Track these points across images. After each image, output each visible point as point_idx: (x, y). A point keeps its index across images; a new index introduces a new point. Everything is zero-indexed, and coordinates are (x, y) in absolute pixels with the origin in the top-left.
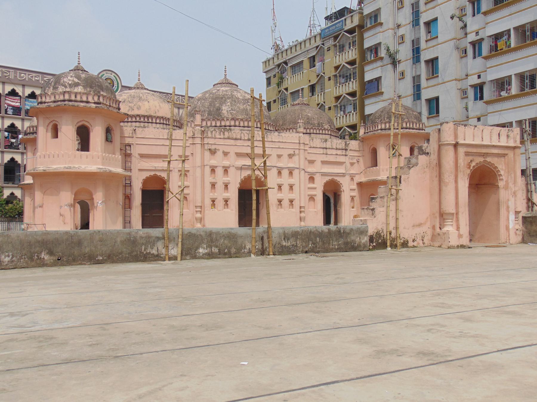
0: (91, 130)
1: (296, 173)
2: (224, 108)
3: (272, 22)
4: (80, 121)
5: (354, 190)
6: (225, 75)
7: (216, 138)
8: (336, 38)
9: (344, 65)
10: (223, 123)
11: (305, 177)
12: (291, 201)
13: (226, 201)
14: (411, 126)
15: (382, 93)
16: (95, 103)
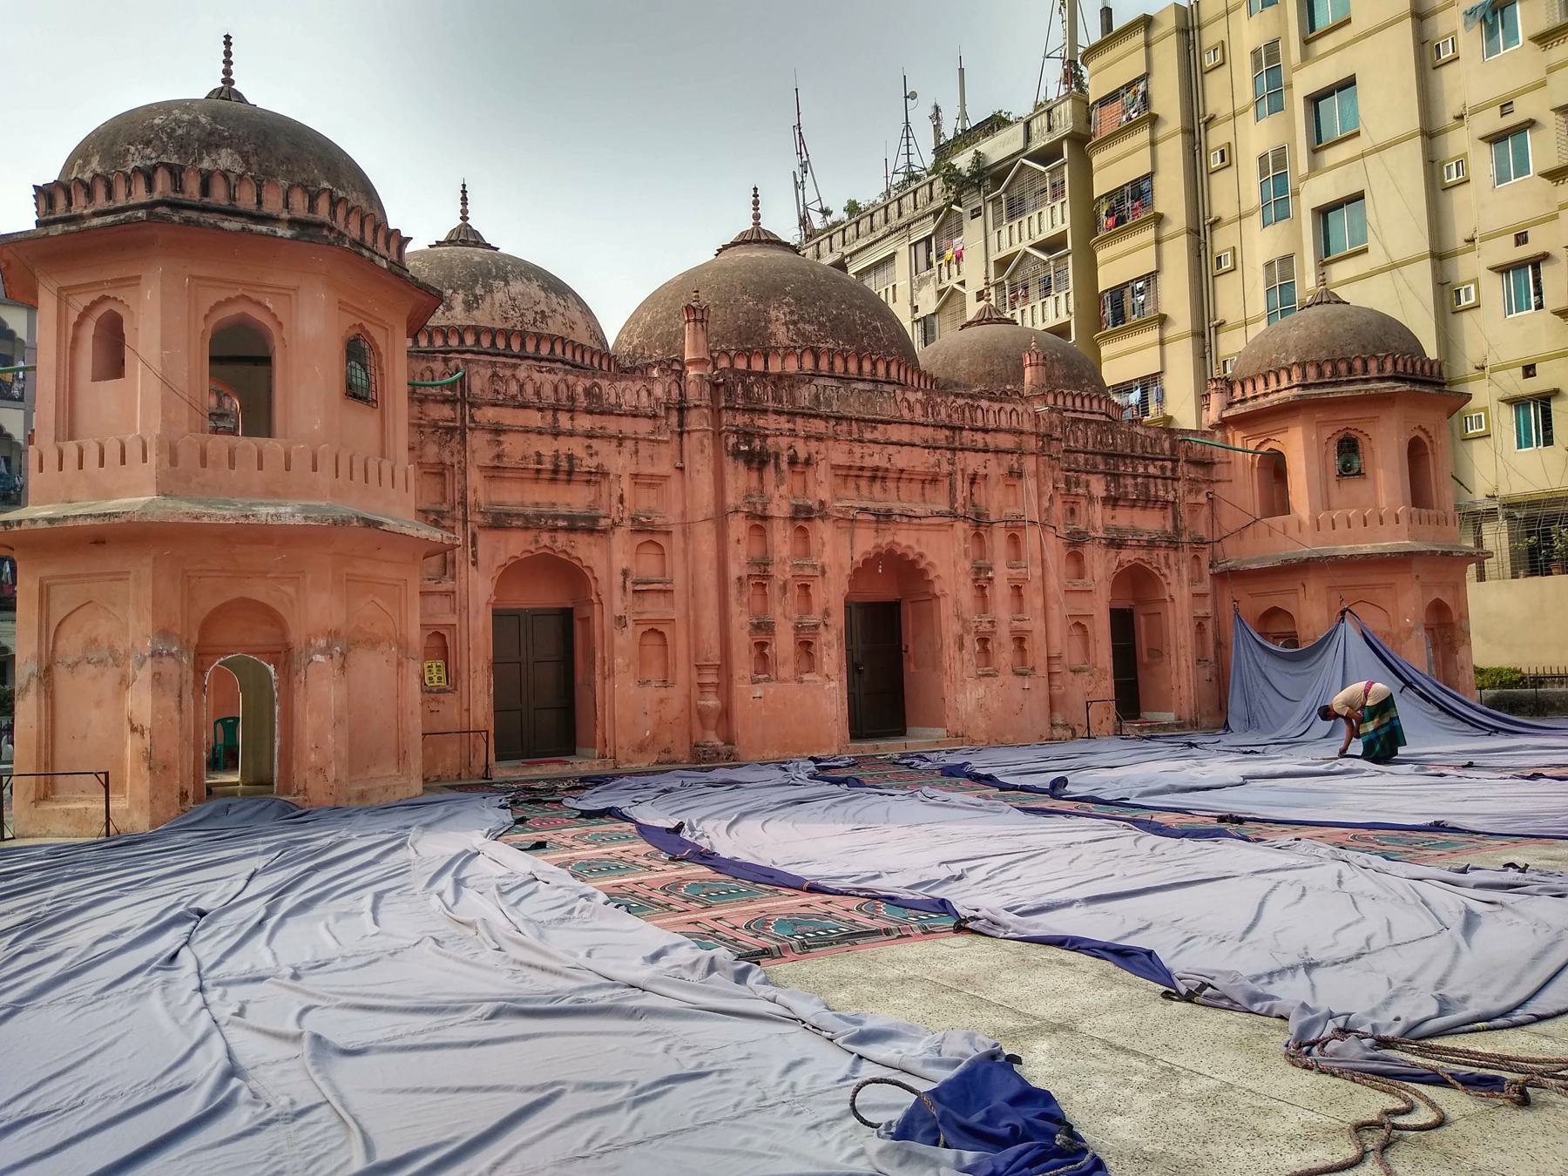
0: (277, 343)
1: (1031, 538)
2: (773, 314)
3: (796, 161)
4: (229, 301)
5: (1205, 595)
6: (757, 217)
7: (765, 411)
8: (998, 178)
9: (1026, 253)
10: (775, 366)
11: (1055, 551)
12: (1020, 640)
13: (806, 647)
14: (1410, 370)
15: (1162, 320)
16: (292, 223)
